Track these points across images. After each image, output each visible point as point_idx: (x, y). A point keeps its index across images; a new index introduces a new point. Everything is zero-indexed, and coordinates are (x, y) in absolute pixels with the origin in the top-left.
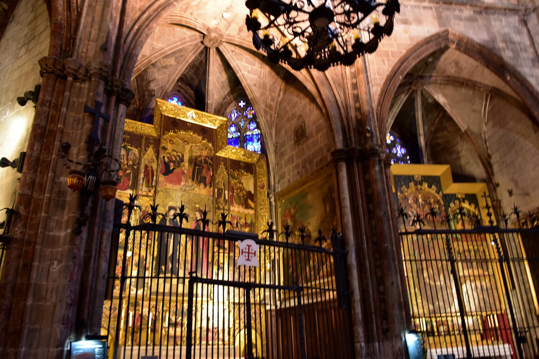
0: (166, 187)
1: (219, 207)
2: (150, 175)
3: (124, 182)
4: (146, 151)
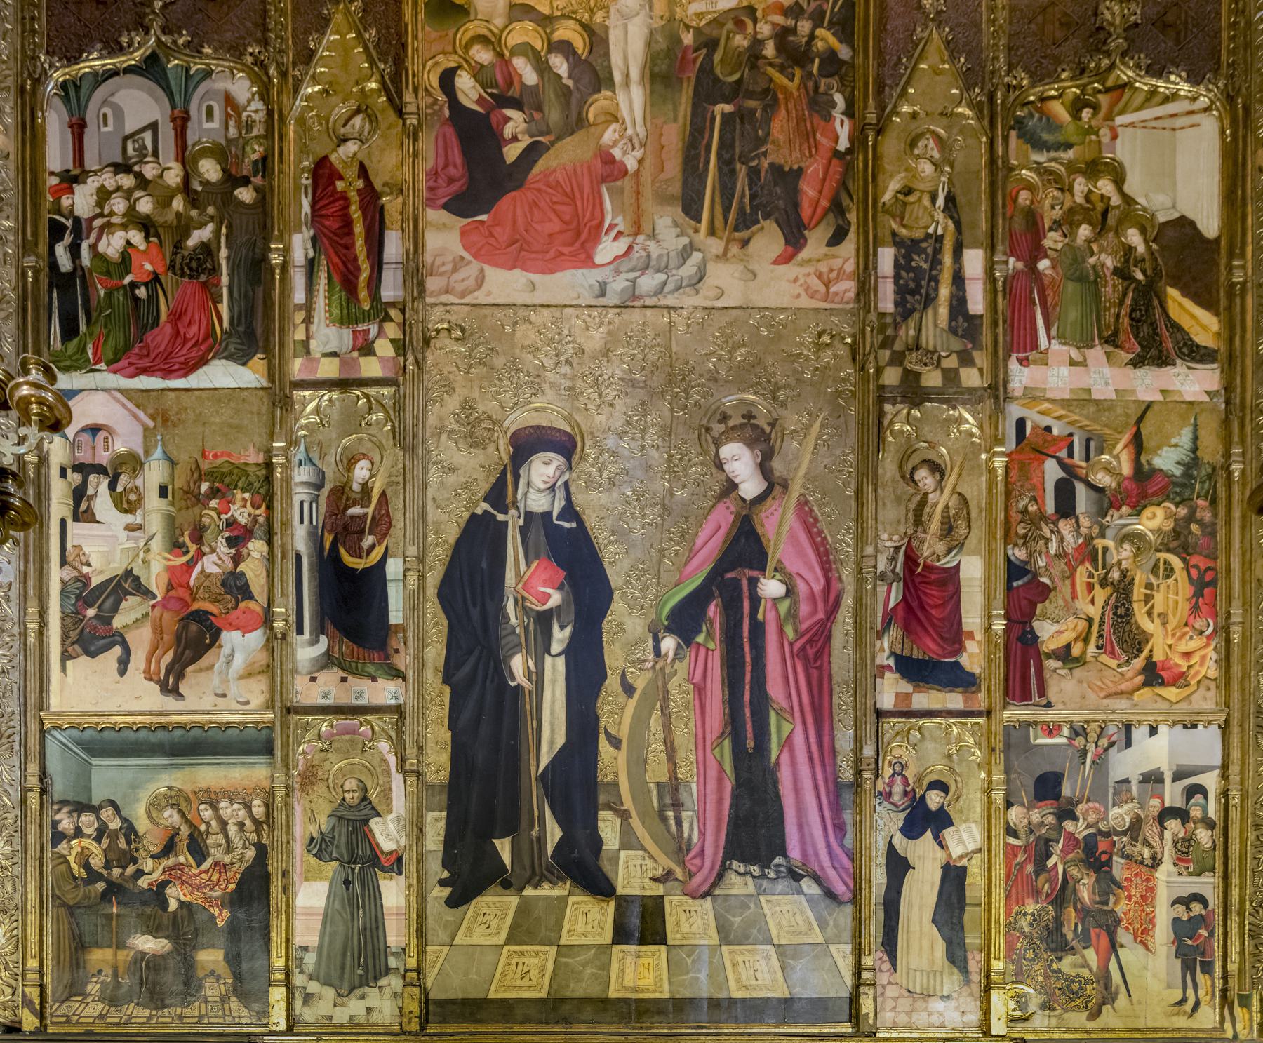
0: (480, 297)
1: (911, 378)
2: (359, 229)
3: (176, 316)
4: (307, 57)
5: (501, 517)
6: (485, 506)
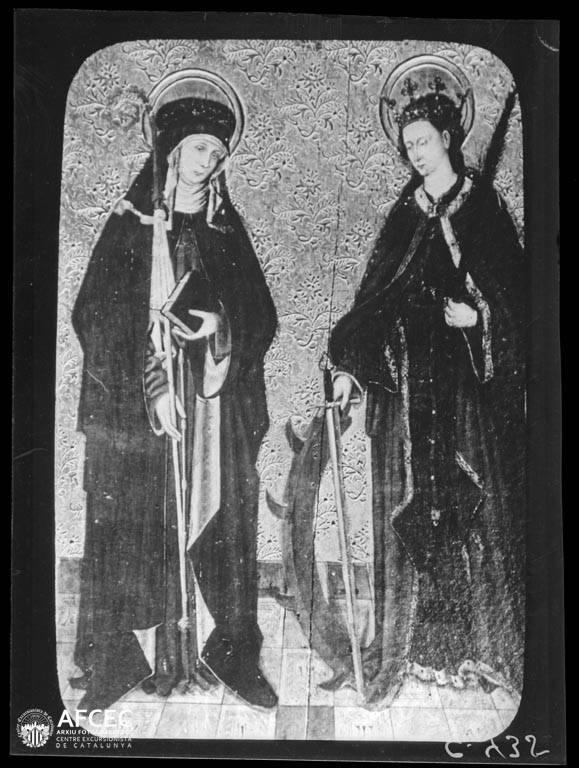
5: (145, 219)
6: (128, 205)
